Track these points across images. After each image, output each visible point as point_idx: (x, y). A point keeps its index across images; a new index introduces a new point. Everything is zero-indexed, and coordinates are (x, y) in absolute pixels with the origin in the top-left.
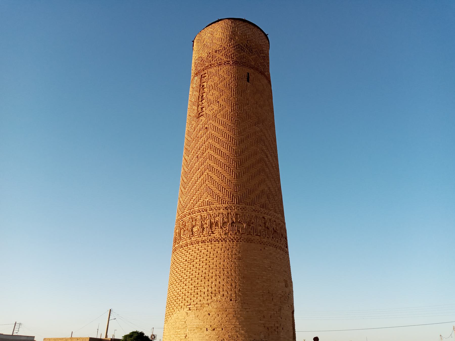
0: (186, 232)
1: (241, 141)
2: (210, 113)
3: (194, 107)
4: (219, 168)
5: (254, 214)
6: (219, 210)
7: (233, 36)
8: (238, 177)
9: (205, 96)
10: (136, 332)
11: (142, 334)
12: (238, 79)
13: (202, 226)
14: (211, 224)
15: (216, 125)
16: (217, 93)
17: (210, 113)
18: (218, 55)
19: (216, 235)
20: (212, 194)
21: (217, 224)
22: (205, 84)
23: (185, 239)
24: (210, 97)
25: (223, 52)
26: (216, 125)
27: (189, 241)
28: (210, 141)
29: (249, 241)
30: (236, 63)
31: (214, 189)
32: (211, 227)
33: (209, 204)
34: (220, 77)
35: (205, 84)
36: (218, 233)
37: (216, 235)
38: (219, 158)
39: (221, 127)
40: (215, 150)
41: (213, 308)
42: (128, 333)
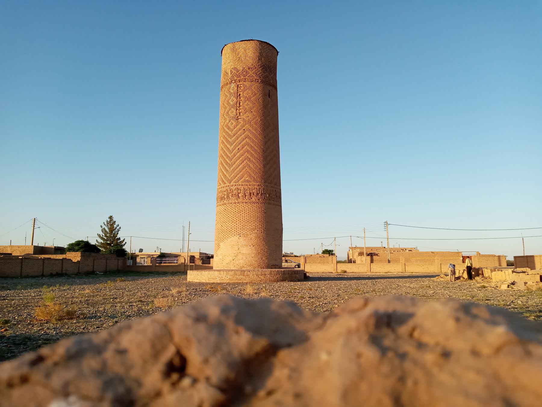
0: (234, 196)
1: (266, 143)
2: (247, 119)
3: (232, 109)
5: (272, 189)
6: (255, 186)
7: (261, 56)
8: (264, 166)
9: (241, 104)
10: (82, 241)
11: (87, 244)
12: (264, 95)
14: (250, 193)
15: (251, 128)
16: (251, 105)
17: (247, 119)
18: (251, 73)
20: (250, 176)
21: (253, 194)
22: (241, 93)
23: (233, 200)
24: (246, 107)
25: (254, 71)
26: (251, 128)
27: (237, 201)
29: (269, 204)
30: (262, 82)
31: (251, 173)
32: (250, 195)
33: (248, 181)
34: (252, 90)
35: (241, 93)
36: (254, 199)
37: (253, 199)
38: (253, 153)
40: (251, 147)
41: (253, 236)
42: (73, 241)
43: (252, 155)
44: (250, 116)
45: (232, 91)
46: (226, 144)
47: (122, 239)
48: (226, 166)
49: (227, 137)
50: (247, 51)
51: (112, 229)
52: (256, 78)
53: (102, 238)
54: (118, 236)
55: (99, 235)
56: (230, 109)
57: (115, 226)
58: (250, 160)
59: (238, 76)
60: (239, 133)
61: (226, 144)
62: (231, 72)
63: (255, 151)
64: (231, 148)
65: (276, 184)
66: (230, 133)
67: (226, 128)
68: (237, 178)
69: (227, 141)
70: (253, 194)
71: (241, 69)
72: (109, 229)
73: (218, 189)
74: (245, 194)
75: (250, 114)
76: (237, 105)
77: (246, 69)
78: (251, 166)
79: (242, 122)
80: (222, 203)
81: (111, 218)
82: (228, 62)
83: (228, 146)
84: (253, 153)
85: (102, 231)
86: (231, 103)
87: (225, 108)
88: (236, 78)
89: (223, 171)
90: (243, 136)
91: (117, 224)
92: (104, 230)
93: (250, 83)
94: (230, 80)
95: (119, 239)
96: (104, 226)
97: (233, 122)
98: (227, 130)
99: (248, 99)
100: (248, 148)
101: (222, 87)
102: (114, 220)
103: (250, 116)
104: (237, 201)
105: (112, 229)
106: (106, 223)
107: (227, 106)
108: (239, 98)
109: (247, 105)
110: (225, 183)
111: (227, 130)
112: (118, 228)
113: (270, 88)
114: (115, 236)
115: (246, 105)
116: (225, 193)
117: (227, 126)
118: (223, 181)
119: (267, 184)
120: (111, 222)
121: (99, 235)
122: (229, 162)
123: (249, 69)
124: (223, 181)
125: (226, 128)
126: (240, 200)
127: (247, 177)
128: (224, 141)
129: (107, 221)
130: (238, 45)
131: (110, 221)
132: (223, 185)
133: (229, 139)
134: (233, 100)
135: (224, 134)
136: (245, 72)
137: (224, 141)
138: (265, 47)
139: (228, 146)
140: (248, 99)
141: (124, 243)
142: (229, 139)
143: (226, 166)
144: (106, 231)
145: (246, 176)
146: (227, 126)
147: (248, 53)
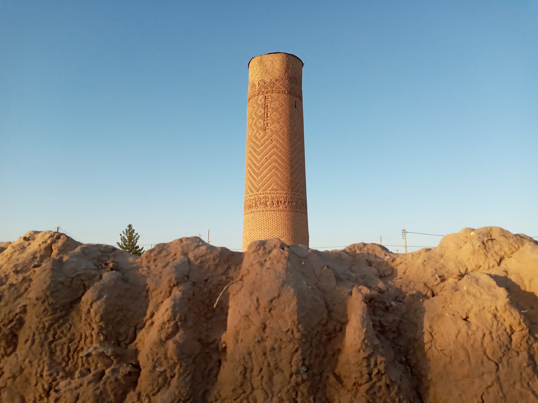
2: (274, 129)
3: (260, 120)
4: (281, 169)
6: (282, 195)
8: (291, 174)
9: (269, 115)
12: (291, 106)
13: (272, 202)
14: (278, 202)
15: (278, 138)
17: (274, 129)
18: (278, 84)
19: (281, 207)
21: (281, 202)
23: (261, 208)
24: (273, 117)
27: (264, 210)
28: (275, 150)
29: (296, 211)
30: (289, 93)
32: (278, 204)
33: (275, 190)
34: (278, 101)
37: (281, 207)
38: (281, 162)
39: (281, 141)
43: (279, 164)
44: (277, 127)
45: (259, 103)
46: (254, 154)
47: (140, 248)
48: (254, 175)
49: (255, 147)
50: (275, 64)
51: (131, 238)
52: (283, 89)
53: (121, 247)
54: (137, 245)
55: (118, 244)
56: (258, 120)
57: (134, 234)
58: (277, 169)
59: (265, 88)
60: (266, 143)
61: (254, 154)
62: (259, 84)
63: (282, 160)
64: (258, 158)
65: (302, 192)
66: (258, 143)
67: (253, 139)
68: (265, 186)
69: (255, 151)
70: (281, 202)
71: (269, 80)
72: (129, 237)
73: (246, 198)
74: (272, 202)
75: (277, 125)
76: (265, 116)
77: (274, 80)
78: (279, 174)
79: (270, 133)
80: (250, 211)
81: (130, 226)
82: (255, 74)
83: (256, 156)
84: (281, 162)
85: (122, 240)
86: (259, 114)
87: (253, 119)
88: (263, 90)
89: (251, 179)
90: (271, 145)
91: (135, 232)
92: (123, 239)
93: (277, 95)
94: (257, 92)
95: (138, 247)
96: (123, 235)
97: (261, 132)
98: (255, 140)
99: (276, 110)
100: (276, 158)
101: (249, 99)
102: (133, 228)
103: (277, 127)
104: (264, 210)
105: (131, 238)
106: (125, 232)
107: (254, 117)
108: (266, 109)
109: (275, 116)
110: (253, 192)
111: (255, 140)
112: (137, 236)
113: (296, 99)
114: (134, 244)
115: (274, 115)
116: (253, 201)
117: (255, 136)
118: (251, 190)
119: (293, 193)
120: (130, 231)
121: (118, 244)
122: (257, 171)
123: (276, 81)
124: (251, 190)
125: (253, 139)
126: (268, 208)
127: (274, 186)
128: (252, 151)
129: (126, 230)
130: (265, 58)
131: (129, 229)
132: (250, 194)
133: (257, 149)
134: (261, 111)
135: (252, 144)
136: (272, 84)
137: (252, 151)
138: (292, 59)
139: (256, 156)
140: (276, 110)
141: (143, 251)
142: (257, 149)
143: (254, 175)
144: (125, 239)
145: (273, 185)
146: (255, 136)
147: (275, 66)
